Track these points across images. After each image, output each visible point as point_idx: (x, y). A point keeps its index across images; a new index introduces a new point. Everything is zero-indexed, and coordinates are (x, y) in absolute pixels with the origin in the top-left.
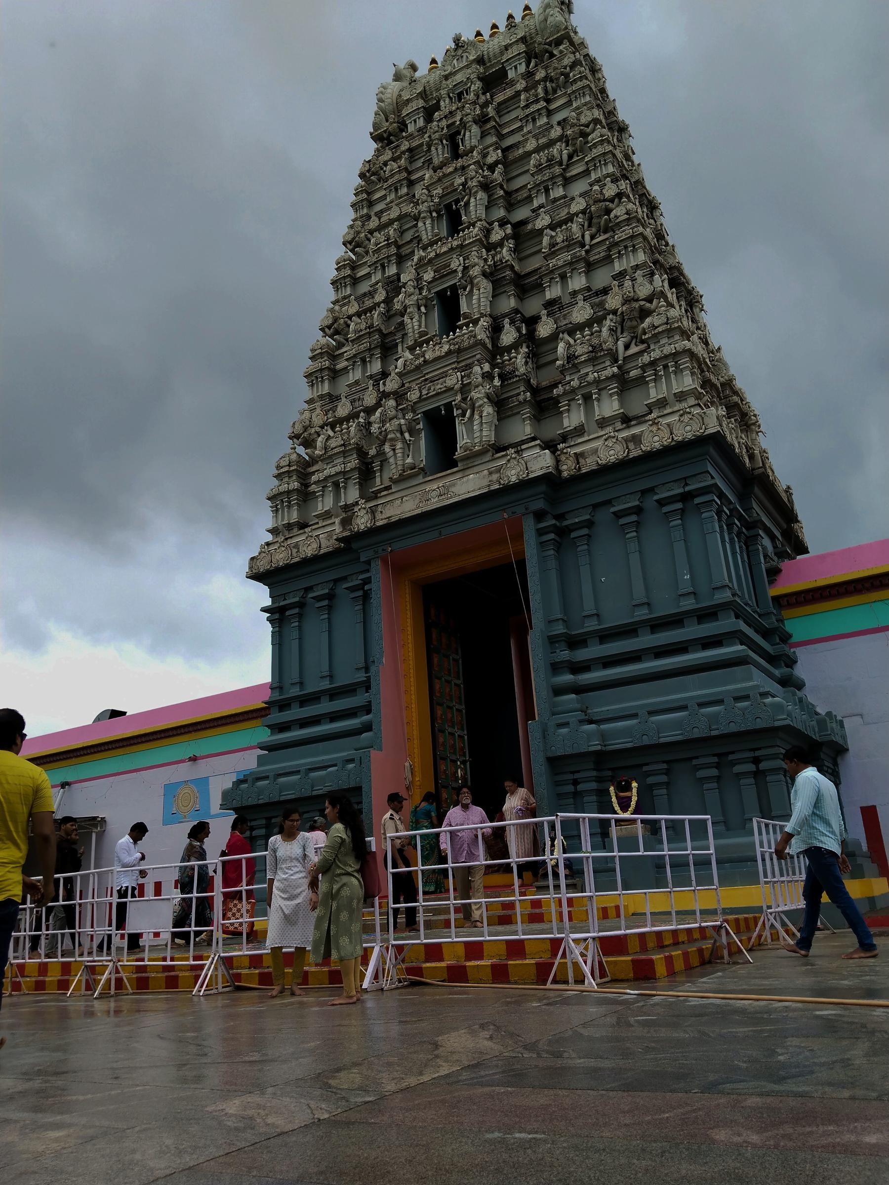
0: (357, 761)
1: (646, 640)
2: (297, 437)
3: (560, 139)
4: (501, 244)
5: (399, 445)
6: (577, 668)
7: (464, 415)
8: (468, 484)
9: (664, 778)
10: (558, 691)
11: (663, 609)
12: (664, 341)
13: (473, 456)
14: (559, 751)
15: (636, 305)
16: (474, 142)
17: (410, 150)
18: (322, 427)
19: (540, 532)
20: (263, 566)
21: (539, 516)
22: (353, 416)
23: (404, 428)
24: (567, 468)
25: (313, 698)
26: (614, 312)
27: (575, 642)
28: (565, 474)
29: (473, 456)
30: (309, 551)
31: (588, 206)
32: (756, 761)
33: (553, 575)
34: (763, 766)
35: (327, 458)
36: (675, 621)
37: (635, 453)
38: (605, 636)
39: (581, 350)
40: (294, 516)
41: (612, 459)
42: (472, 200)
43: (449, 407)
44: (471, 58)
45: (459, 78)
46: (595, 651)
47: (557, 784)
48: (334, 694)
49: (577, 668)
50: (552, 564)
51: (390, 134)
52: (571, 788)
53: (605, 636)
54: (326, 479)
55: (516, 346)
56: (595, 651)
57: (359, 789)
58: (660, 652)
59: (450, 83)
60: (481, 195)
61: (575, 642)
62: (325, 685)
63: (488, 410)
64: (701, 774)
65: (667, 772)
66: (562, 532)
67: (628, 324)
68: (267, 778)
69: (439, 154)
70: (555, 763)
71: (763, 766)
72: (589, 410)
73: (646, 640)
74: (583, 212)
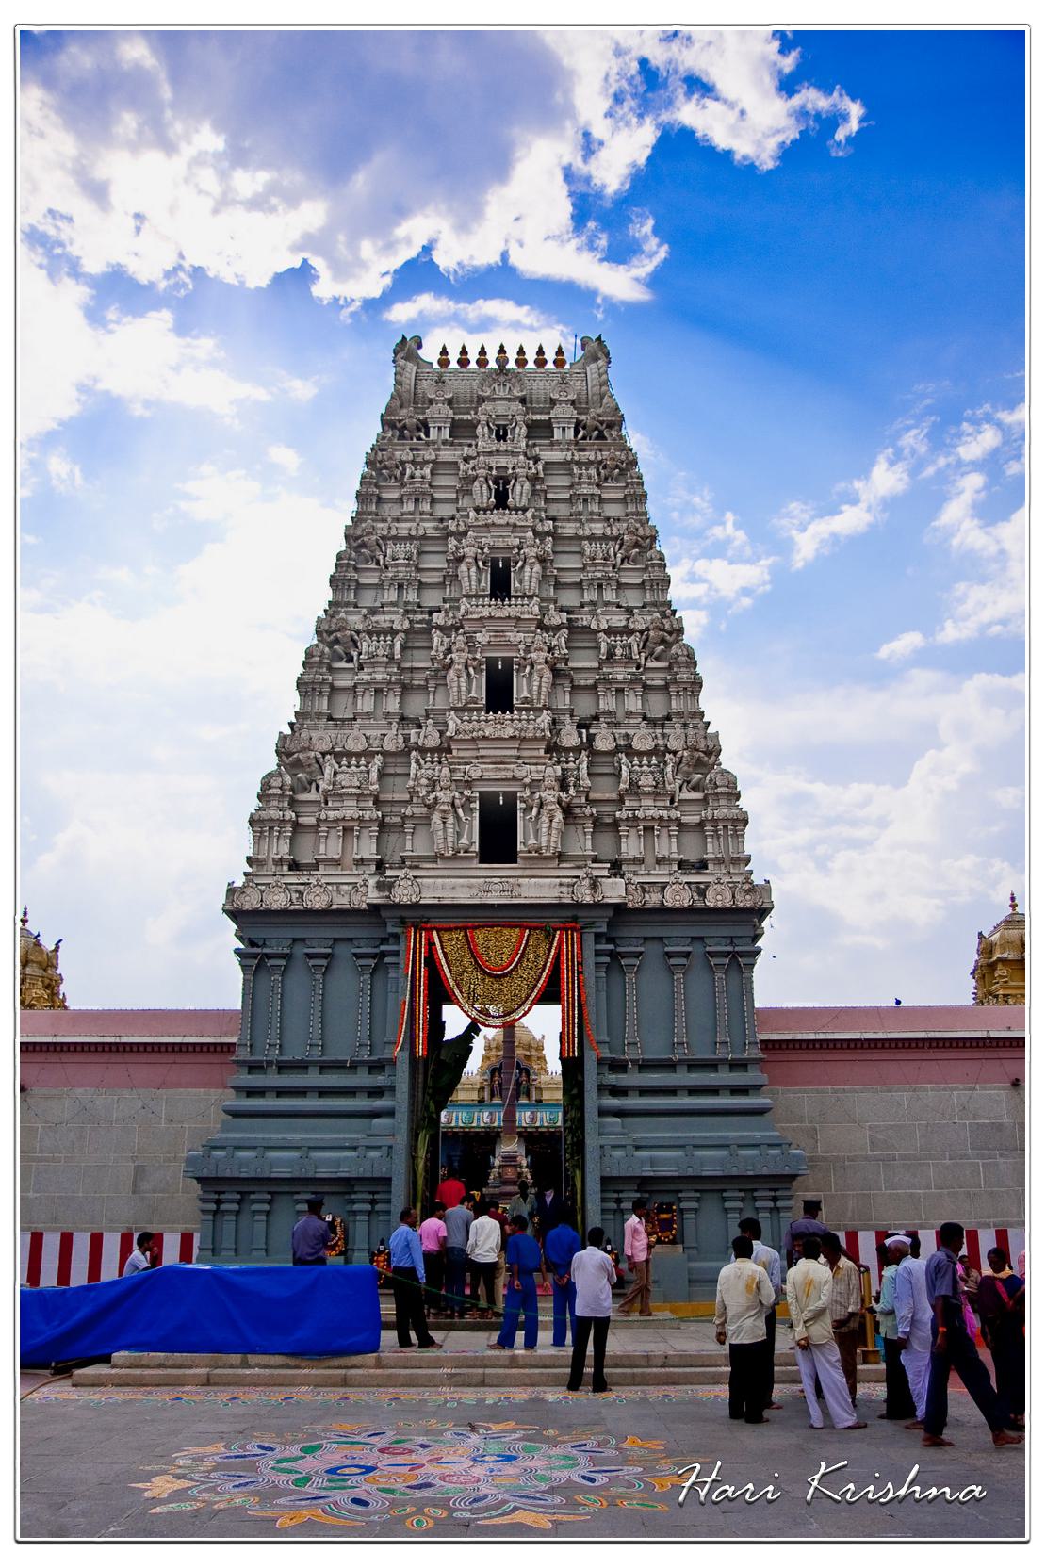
0: (385, 1149)
1: (682, 1077)
2: (289, 754)
3: (616, 539)
4: (558, 628)
5: (451, 820)
6: (617, 1091)
7: (528, 809)
8: (538, 888)
9: (694, 1205)
10: (603, 1112)
11: (703, 1054)
12: (723, 802)
13: (538, 857)
14: (608, 1172)
15: (697, 754)
16: (524, 502)
17: (434, 462)
18: (324, 754)
19: (598, 953)
20: (250, 902)
21: (598, 937)
22: (368, 754)
23: (457, 802)
24: (634, 901)
25: (302, 1066)
26: (675, 753)
27: (617, 1066)
28: (630, 905)
29: (538, 857)
30: (317, 901)
31: (647, 629)
32: (775, 1199)
33: (603, 995)
34: (780, 1204)
35: (334, 794)
36: (712, 1066)
37: (700, 905)
38: (645, 1066)
39: (646, 782)
40: (283, 849)
41: (678, 904)
42: (527, 569)
43: (512, 798)
44: (516, 393)
45: (501, 408)
46: (632, 1078)
47: (603, 1200)
48: (325, 1067)
49: (617, 1091)
50: (603, 985)
51: (405, 427)
52: (613, 1206)
53: (645, 1066)
54: (336, 821)
55: (577, 750)
56: (632, 1078)
57: (390, 1179)
58: (694, 1091)
59: (487, 406)
60: (537, 568)
61: (617, 1066)
62: (316, 1054)
63: (559, 816)
64: (727, 1205)
65: (698, 1200)
66: (614, 956)
67: (684, 767)
68: (223, 1148)
69: (483, 494)
70: (606, 1181)
71: (780, 1204)
72: (649, 846)
73: (682, 1077)
74: (641, 632)
